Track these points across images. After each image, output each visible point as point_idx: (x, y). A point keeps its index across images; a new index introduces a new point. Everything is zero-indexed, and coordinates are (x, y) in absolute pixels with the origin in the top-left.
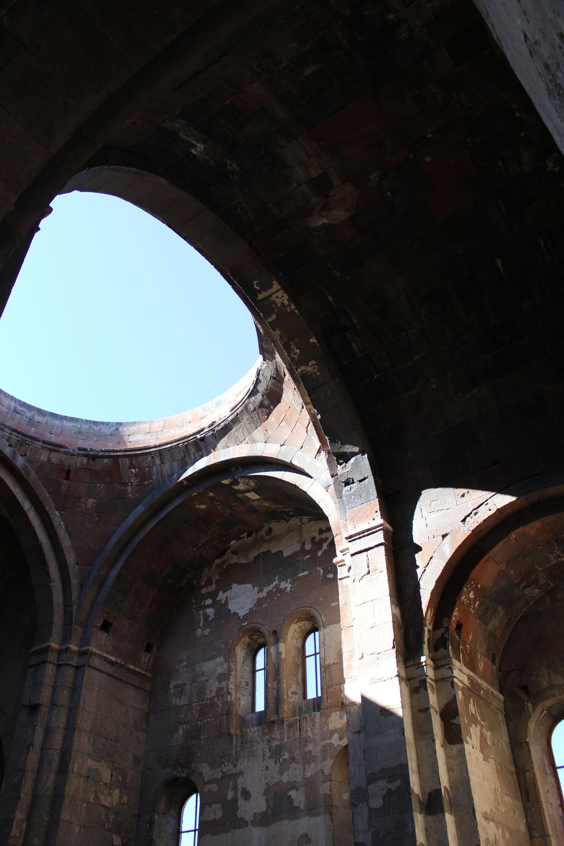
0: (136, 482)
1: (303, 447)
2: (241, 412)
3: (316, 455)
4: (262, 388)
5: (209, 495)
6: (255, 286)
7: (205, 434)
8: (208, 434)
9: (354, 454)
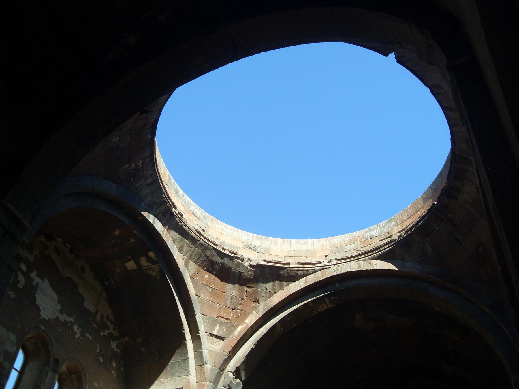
0: (132, 170)
1: (204, 316)
2: (200, 243)
3: (208, 333)
4: (226, 261)
5: (132, 239)
6: (334, 297)
7: (176, 216)
8: (177, 218)
9: (241, 379)
